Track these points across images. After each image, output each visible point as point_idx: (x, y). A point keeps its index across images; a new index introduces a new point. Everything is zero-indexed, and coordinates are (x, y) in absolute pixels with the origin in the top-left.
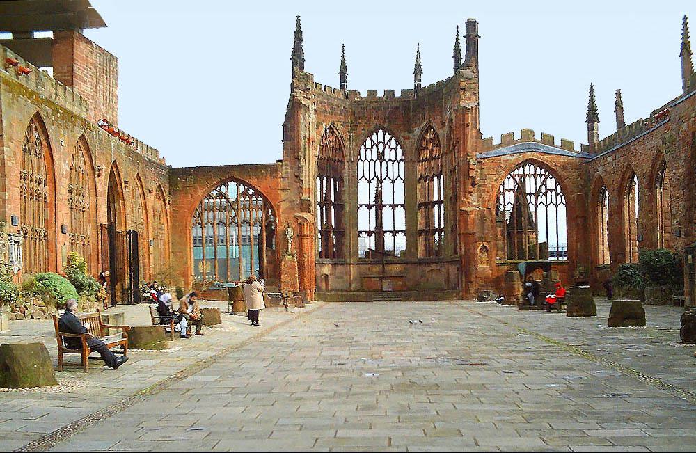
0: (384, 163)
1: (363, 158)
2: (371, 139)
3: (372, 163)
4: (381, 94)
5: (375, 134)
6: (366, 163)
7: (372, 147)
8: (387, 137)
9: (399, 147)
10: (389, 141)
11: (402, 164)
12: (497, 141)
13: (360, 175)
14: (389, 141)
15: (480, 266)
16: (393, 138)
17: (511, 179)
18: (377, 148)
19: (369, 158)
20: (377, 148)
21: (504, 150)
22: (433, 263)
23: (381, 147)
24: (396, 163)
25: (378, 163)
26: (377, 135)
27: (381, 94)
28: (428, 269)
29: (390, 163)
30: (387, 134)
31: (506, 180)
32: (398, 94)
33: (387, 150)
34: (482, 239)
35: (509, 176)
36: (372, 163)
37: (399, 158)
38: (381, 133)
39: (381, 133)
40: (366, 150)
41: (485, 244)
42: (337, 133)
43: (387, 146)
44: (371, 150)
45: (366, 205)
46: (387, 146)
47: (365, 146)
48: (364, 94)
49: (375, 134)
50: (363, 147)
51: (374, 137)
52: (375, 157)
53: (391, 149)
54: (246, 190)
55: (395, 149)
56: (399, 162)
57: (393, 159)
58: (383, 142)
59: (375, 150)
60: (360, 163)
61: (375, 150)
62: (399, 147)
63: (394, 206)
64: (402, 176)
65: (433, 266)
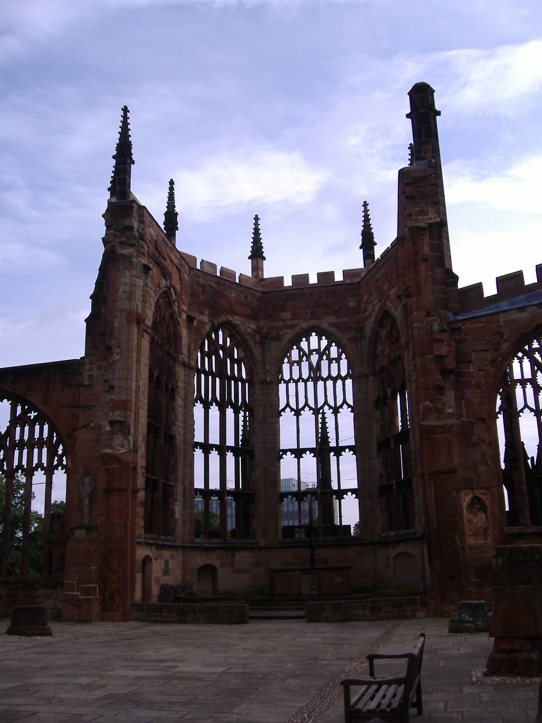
0: (320, 384)
1: (286, 377)
2: (300, 349)
3: (301, 385)
4: (313, 280)
5: (304, 339)
6: (292, 386)
7: (301, 358)
8: (324, 343)
9: (343, 356)
10: (328, 348)
11: (349, 382)
12: (490, 290)
13: (282, 405)
14: (328, 348)
15: (471, 541)
16: (334, 344)
17: (526, 363)
18: (308, 359)
19: (296, 376)
20: (308, 359)
21: (504, 305)
22: (399, 542)
23: (314, 358)
24: (339, 382)
25: (310, 384)
26: (308, 340)
27: (313, 280)
28: (393, 552)
29: (330, 383)
30: (324, 338)
31: (516, 364)
32: (339, 277)
33: (324, 363)
34: (469, 485)
35: (520, 354)
36: (301, 385)
37: (344, 373)
38: (314, 338)
39: (314, 338)
40: (291, 363)
41: (478, 493)
42: (239, 338)
43: (325, 357)
44: (299, 363)
45: (292, 451)
46: (325, 357)
47: (289, 358)
48: (288, 282)
49: (304, 339)
50: (286, 360)
51: (304, 344)
52: (305, 376)
53: (330, 361)
54: (24, 412)
55: (338, 360)
56: (344, 379)
57: (334, 374)
58: (318, 351)
59: (305, 365)
60: (282, 387)
61: (305, 365)
62: (343, 356)
63: (339, 451)
64: (350, 401)
65: (401, 548)
